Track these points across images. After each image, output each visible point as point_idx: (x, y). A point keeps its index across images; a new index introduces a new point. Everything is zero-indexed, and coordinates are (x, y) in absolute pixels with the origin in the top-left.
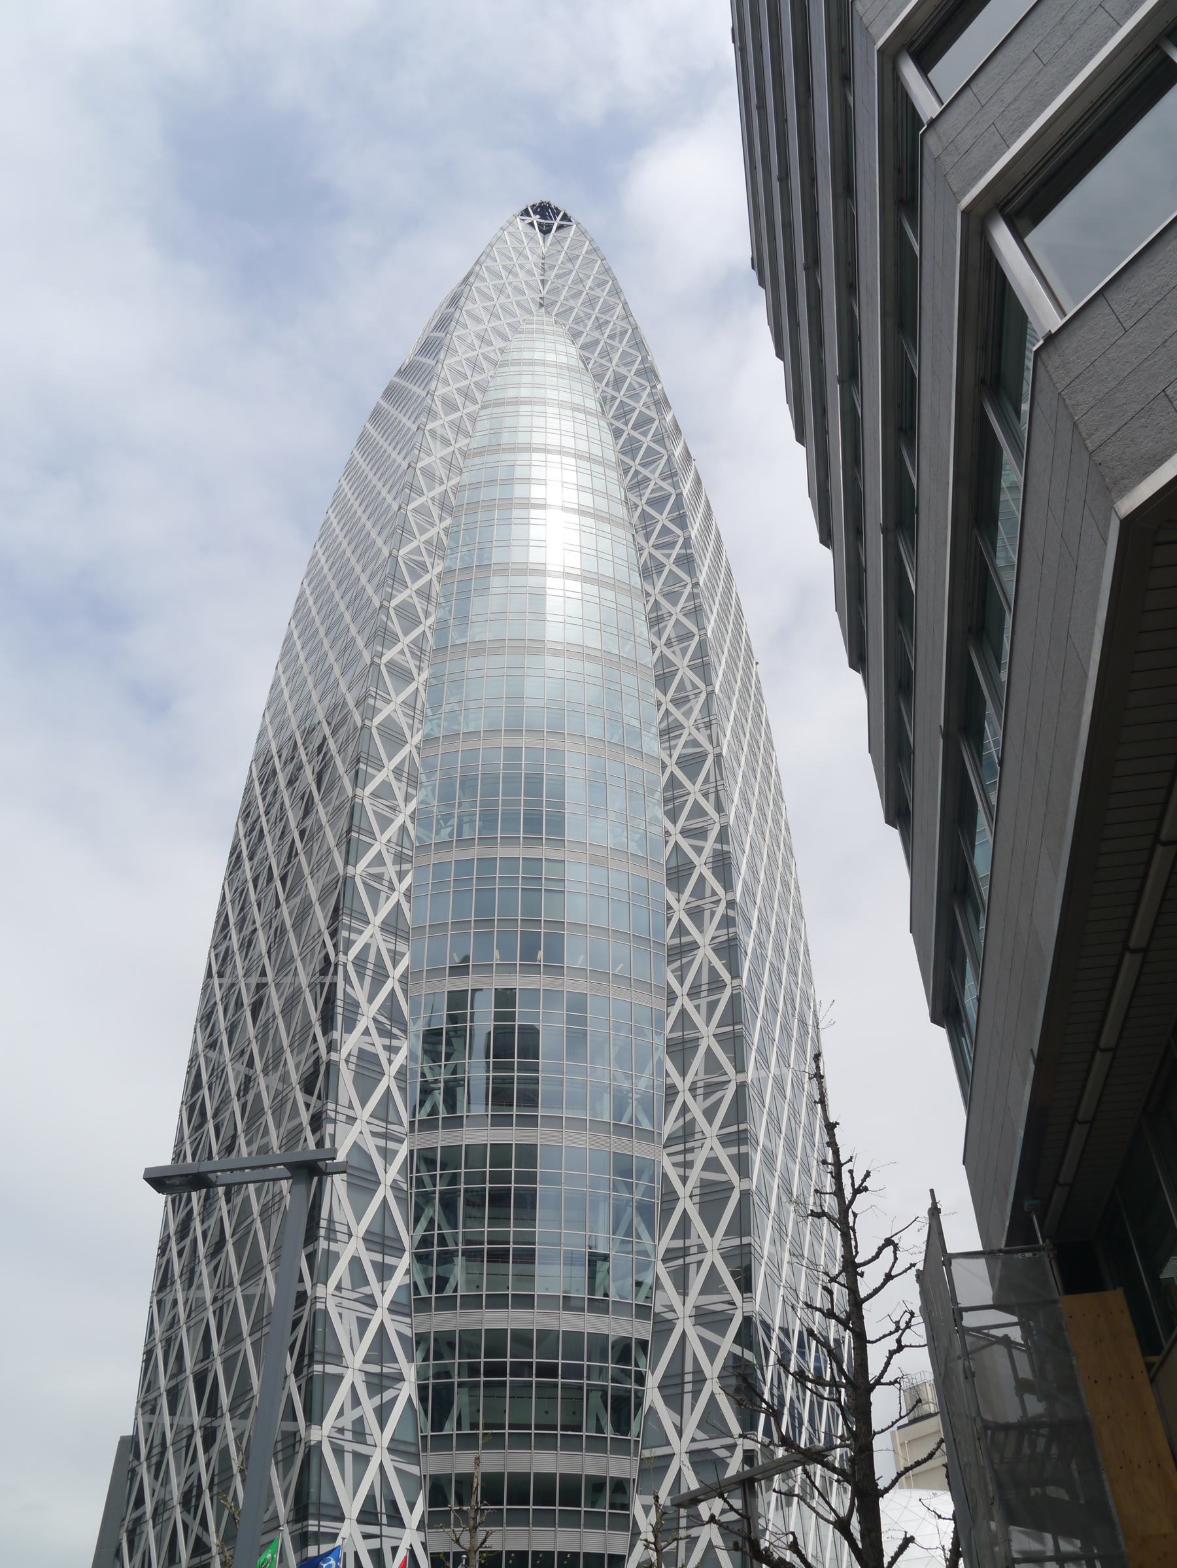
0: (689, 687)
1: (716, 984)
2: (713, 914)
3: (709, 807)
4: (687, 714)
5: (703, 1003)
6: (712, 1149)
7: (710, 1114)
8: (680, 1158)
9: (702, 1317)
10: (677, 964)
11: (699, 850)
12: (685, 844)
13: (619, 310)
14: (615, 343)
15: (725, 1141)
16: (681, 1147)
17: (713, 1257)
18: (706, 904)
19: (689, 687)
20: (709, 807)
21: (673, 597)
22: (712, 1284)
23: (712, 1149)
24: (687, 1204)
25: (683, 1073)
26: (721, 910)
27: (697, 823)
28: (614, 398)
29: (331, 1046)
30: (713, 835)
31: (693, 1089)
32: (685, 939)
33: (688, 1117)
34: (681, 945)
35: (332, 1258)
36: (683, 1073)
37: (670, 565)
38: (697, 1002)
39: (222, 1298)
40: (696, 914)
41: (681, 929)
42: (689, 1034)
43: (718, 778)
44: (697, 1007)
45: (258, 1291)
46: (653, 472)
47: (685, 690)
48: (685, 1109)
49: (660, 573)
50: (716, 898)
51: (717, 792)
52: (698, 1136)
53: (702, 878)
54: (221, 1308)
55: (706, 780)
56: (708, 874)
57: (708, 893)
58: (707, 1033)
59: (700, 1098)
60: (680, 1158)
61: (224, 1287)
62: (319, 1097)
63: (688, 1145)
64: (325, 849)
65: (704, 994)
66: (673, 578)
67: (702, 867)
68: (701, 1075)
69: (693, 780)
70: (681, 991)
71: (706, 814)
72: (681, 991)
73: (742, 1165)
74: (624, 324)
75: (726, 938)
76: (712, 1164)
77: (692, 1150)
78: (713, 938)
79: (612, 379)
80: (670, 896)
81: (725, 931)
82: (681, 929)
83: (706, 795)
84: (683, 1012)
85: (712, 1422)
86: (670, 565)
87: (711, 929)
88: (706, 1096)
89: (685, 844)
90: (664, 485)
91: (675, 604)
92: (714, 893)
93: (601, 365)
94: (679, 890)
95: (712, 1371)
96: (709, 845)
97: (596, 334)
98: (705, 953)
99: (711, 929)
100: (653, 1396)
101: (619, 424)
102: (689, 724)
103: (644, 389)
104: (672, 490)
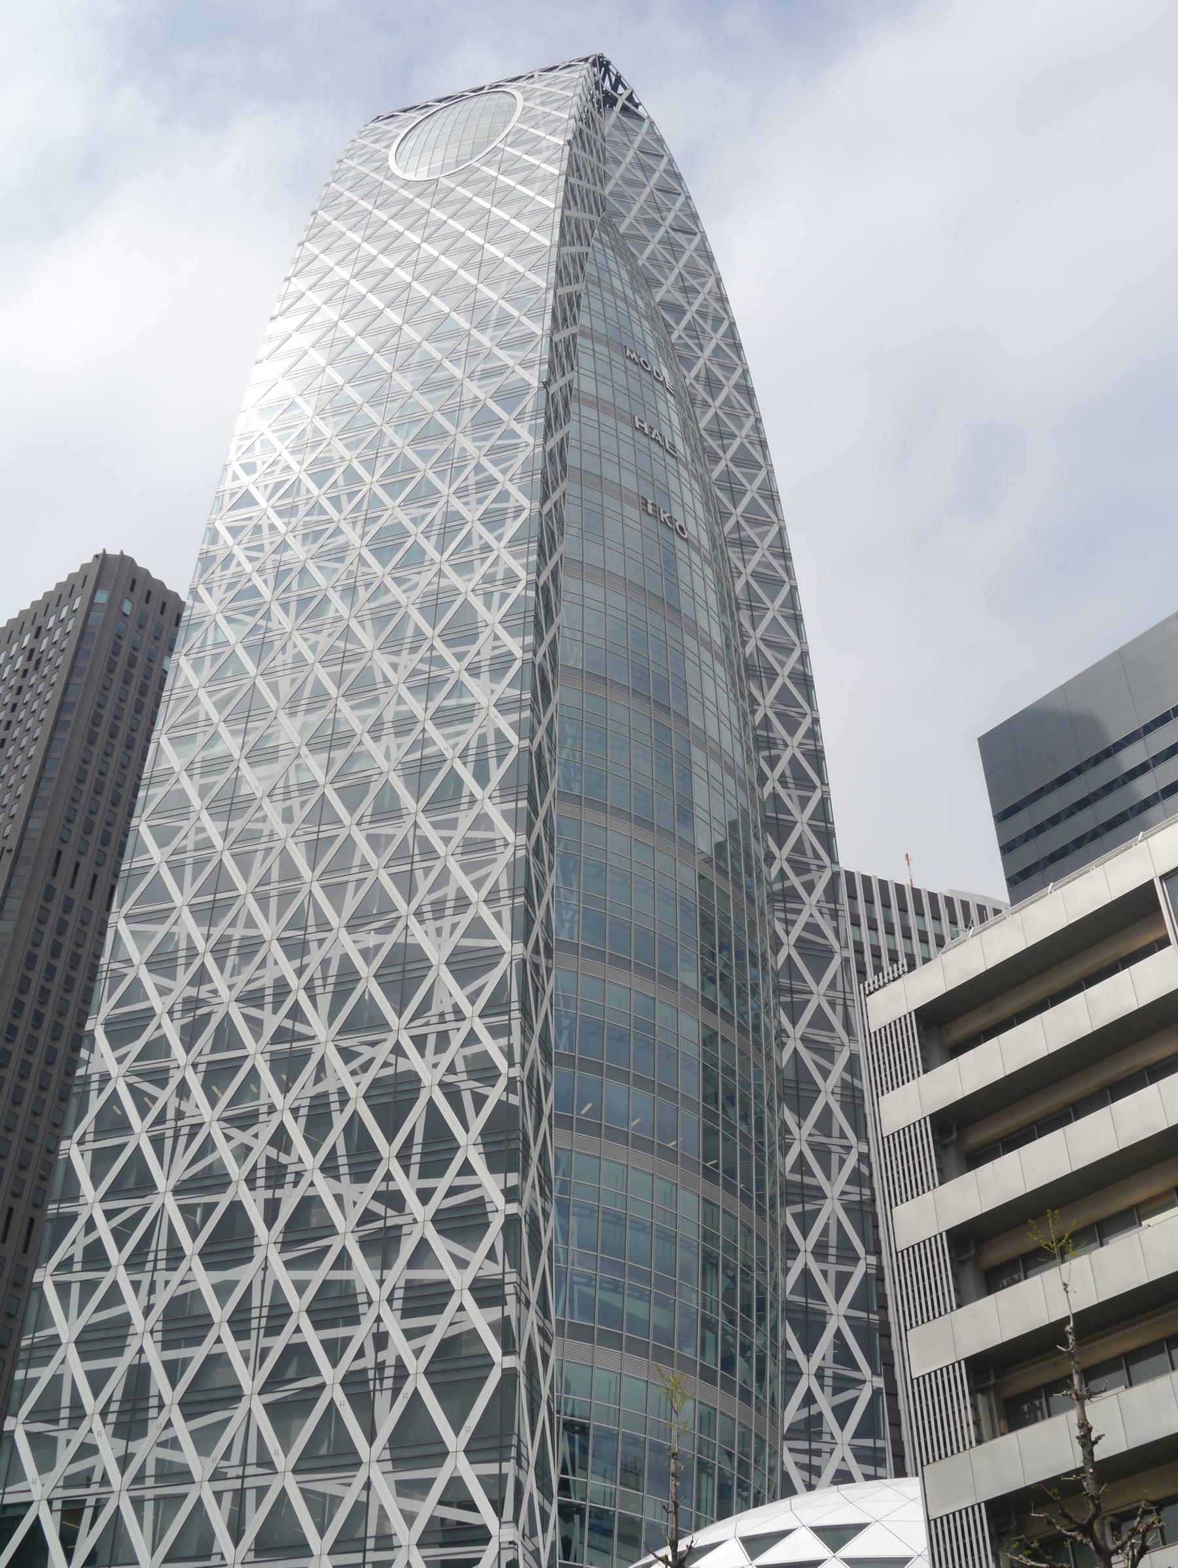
0: (810, 853)
1: (847, 1255)
2: (842, 1162)
3: (836, 1021)
4: (810, 887)
5: (833, 1269)
6: (843, 1459)
7: (842, 1413)
8: (805, 1459)
10: (798, 1208)
11: (826, 1074)
12: (806, 1055)
13: (711, 281)
14: (707, 327)
16: (804, 1445)
18: (834, 1142)
19: (810, 853)
20: (836, 1021)
21: (792, 726)
23: (843, 1459)
25: (808, 1350)
26: (852, 1161)
27: (821, 1036)
28: (706, 405)
30: (842, 1059)
31: (820, 1375)
32: (808, 1180)
33: (814, 1410)
34: (802, 1186)
36: (808, 1350)
38: (824, 1266)
39: (243, 1477)
41: (801, 1164)
42: (814, 1304)
43: (848, 990)
44: (825, 1273)
45: (351, 1496)
47: (804, 853)
48: (809, 1399)
49: (771, 682)
50: (843, 1142)
51: (845, 1006)
52: (826, 1438)
53: (827, 1108)
54: (240, 1494)
55: (832, 985)
56: (836, 1108)
57: (836, 1132)
58: (838, 1313)
59: (829, 1390)
60: (805, 1459)
61: (244, 1463)
62: (491, 1255)
63: (815, 1446)
64: (450, 892)
65: (832, 1259)
66: (784, 696)
67: (828, 1095)
68: (830, 1362)
70: (806, 1245)
71: (833, 1030)
72: (806, 1245)
74: (717, 306)
75: (857, 1198)
77: (818, 1453)
78: (843, 1193)
79: (703, 374)
80: (790, 1118)
81: (857, 1190)
82: (801, 1164)
83: (832, 1004)
84: (806, 1273)
88: (836, 1391)
89: (806, 1055)
91: (792, 733)
92: (843, 1135)
93: (687, 346)
94: (802, 1114)
96: (838, 1070)
97: (680, 299)
98: (831, 1210)
101: (715, 444)
103: (748, 416)
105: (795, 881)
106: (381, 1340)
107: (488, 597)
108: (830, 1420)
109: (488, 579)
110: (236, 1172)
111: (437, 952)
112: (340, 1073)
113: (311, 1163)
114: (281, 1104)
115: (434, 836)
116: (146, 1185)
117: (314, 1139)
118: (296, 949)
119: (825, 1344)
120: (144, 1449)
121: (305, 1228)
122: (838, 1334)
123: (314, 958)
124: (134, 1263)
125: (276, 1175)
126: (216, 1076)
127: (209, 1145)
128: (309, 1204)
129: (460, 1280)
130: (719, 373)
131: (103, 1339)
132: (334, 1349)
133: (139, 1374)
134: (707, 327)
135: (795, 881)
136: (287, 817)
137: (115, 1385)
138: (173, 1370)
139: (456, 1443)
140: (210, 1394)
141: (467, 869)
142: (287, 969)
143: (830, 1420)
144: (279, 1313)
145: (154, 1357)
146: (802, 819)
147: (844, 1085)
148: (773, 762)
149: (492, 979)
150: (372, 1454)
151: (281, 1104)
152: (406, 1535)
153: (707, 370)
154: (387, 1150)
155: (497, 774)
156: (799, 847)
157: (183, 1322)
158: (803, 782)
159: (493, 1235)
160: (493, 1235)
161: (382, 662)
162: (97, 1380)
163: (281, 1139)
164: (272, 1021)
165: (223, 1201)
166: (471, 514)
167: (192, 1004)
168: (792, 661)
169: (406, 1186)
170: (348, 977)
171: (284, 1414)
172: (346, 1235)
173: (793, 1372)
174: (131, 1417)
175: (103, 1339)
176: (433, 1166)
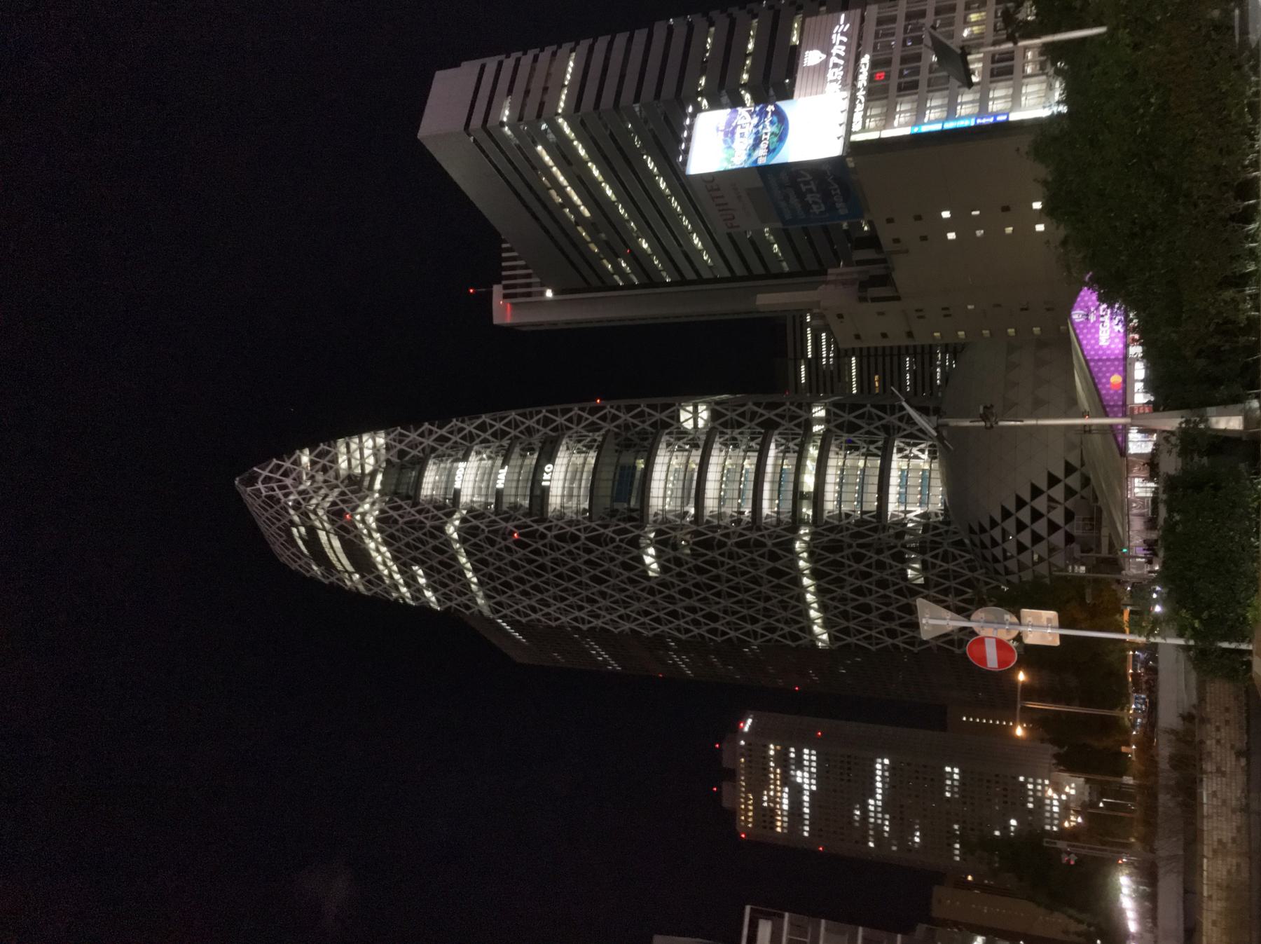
3: (742, 409)
7: (880, 418)
11: (762, 415)
15: (893, 413)
20: (742, 409)
26: (793, 408)
27: (748, 416)
29: (850, 546)
30: (756, 409)
35: (932, 542)
37: (594, 418)
40: (792, 418)
46: (523, 423)
48: (877, 428)
53: (777, 415)
69: (725, 415)
86: (594, 418)
89: (757, 421)
90: (535, 418)
93: (423, 450)
96: (760, 411)
104: (540, 416)
106: (892, 574)
108: (883, 422)
109: (617, 553)
110: (842, 608)
111: (771, 564)
116: (847, 628)
118: (768, 599)
119: (858, 422)
121: (859, 591)
122: (856, 417)
124: (870, 629)
129: (876, 557)
130: (434, 436)
131: (892, 633)
134: (407, 440)
136: (718, 603)
137: (905, 630)
138: (901, 618)
142: (774, 601)
143: (883, 422)
144: (885, 596)
145: (898, 622)
147: (765, 408)
148: (635, 426)
152: (945, 566)
153: (435, 440)
154: (835, 574)
157: (887, 617)
158: (641, 414)
159: (863, 551)
160: (863, 551)
162: (903, 634)
165: (851, 611)
166: (586, 557)
167: (787, 622)
168: (585, 415)
169: (847, 570)
170: (778, 586)
175: (892, 633)
176: (842, 565)
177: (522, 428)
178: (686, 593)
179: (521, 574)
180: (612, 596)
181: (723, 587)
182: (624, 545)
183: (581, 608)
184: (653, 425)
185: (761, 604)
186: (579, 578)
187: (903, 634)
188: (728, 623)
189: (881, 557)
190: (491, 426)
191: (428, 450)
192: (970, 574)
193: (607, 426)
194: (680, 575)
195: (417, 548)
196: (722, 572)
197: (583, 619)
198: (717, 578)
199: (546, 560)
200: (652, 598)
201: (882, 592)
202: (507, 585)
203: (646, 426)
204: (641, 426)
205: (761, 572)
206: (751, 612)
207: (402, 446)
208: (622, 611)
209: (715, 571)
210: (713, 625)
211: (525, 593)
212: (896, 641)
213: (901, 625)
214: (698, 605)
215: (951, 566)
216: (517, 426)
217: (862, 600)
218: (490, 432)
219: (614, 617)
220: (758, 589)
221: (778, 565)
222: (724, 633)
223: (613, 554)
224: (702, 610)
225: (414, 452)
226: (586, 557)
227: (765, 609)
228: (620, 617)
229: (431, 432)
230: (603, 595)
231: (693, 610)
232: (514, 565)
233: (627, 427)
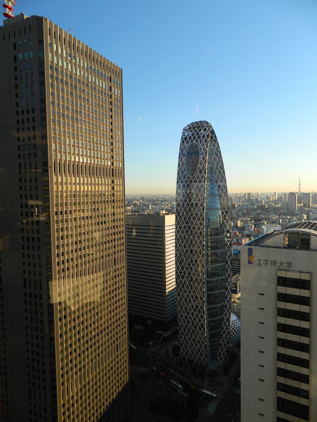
4: (229, 269)
7: (228, 313)
9: (226, 328)
12: (228, 286)
15: (229, 316)
17: (227, 324)
22: (227, 326)
24: (225, 320)
27: (229, 284)
41: (226, 295)
46: (228, 225)
58: (228, 306)
70: (226, 301)
72: (226, 301)
73: (230, 318)
76: (228, 317)
82: (226, 295)
85: (226, 335)
87: (229, 296)
89: (228, 286)
95: (226, 332)
98: (228, 298)
99: (229, 296)
100: (222, 333)
102: (229, 271)
105: (228, 269)
107: (200, 262)
109: (200, 260)
110: (188, 309)
111: (199, 297)
112: (193, 304)
113: (192, 310)
114: (190, 305)
115: (198, 287)
117: (192, 308)
118: (189, 293)
119: (227, 308)
120: (185, 323)
121: (192, 314)
123: (191, 294)
125: (190, 310)
126: (186, 301)
127: (186, 306)
128: (192, 312)
132: (195, 322)
133: (184, 319)
135: (228, 269)
139: (202, 329)
140: (188, 322)
141: (200, 291)
144: (192, 319)
146: (229, 262)
148: (227, 256)
149: (203, 300)
150: (198, 328)
151: (190, 305)
154: (197, 311)
155: (202, 283)
156: (228, 265)
157: (186, 317)
158: (230, 257)
161: (192, 267)
163: (190, 307)
164: (189, 298)
166: (198, 251)
167: (183, 295)
170: (193, 297)
171: (193, 324)
172: (195, 315)
173: (225, 310)
174: (184, 321)
175: (182, 316)
177: (226, 224)
178: (189, 274)
179: (191, 229)
180: (187, 253)
181: (192, 283)
182: (202, 263)
183: (182, 242)
184: (227, 260)
185: (188, 291)
186: (192, 246)
187: (182, 319)
188: (181, 281)
189: (202, 321)
190: (227, 215)
191: (221, 195)
192: (198, 337)
193: (227, 248)
194: (195, 275)
195: (197, 197)
196: (196, 285)
197: (179, 242)
198: (194, 283)
199: (196, 238)
200: (187, 264)
201: (193, 318)
202: (187, 223)
203: (227, 258)
204: (227, 257)
205: (196, 294)
206: (185, 287)
207: (222, 187)
208: (183, 254)
209: (196, 283)
210: (181, 277)
211: (185, 227)
212: (180, 316)
213: (184, 319)
214: (186, 275)
215: (200, 334)
216: (227, 223)
217: (190, 314)
218: (225, 215)
219: (180, 251)
220: (192, 292)
221: (199, 299)
222: (179, 279)
223: (200, 259)
224: (185, 276)
225: (220, 190)
226: (198, 251)
227: (186, 291)
228: (180, 253)
229: (225, 196)
230: (187, 251)
231: (185, 273)
232: (194, 228)
233: (227, 253)
